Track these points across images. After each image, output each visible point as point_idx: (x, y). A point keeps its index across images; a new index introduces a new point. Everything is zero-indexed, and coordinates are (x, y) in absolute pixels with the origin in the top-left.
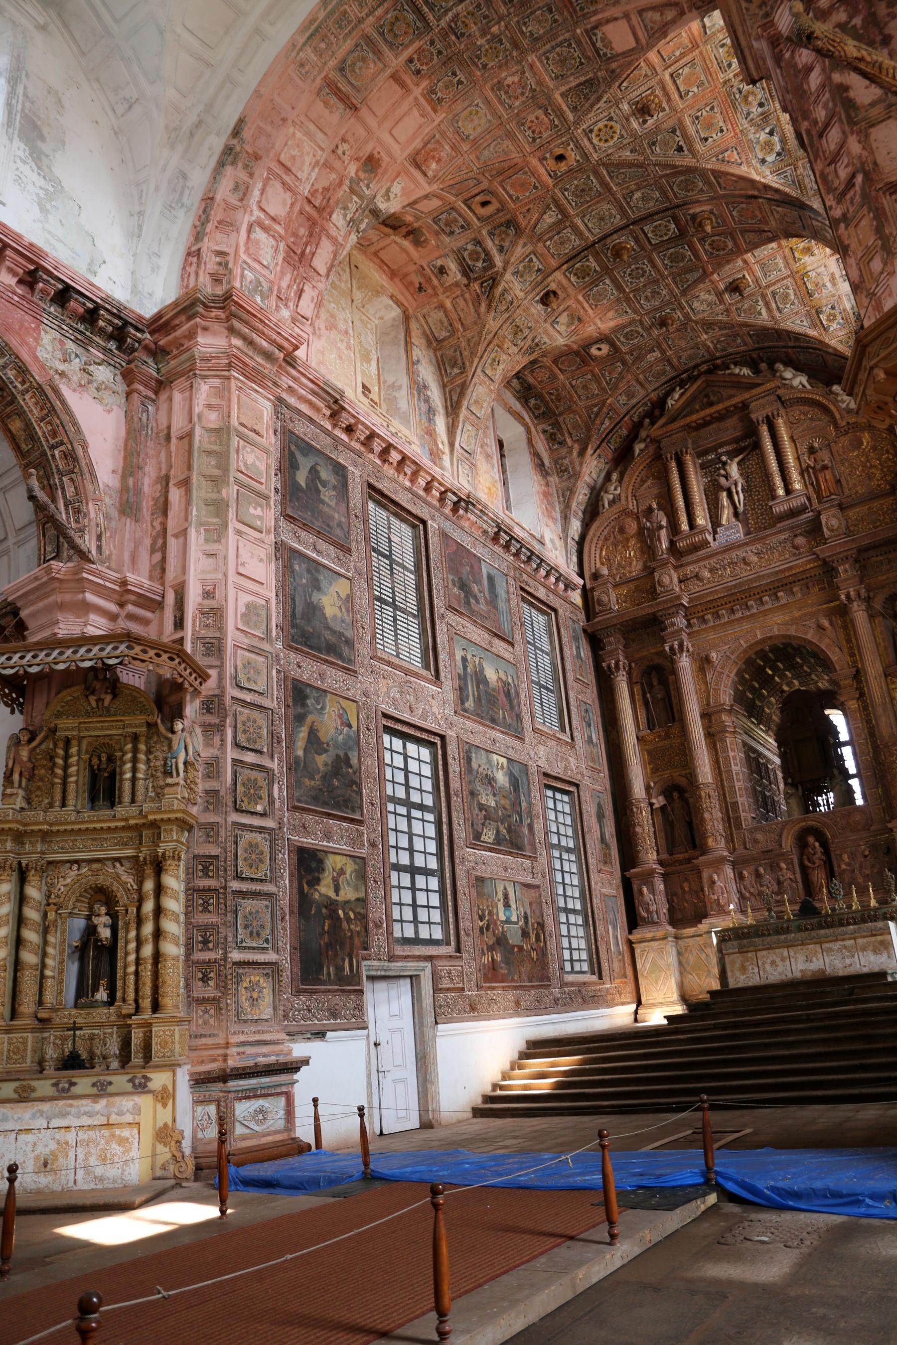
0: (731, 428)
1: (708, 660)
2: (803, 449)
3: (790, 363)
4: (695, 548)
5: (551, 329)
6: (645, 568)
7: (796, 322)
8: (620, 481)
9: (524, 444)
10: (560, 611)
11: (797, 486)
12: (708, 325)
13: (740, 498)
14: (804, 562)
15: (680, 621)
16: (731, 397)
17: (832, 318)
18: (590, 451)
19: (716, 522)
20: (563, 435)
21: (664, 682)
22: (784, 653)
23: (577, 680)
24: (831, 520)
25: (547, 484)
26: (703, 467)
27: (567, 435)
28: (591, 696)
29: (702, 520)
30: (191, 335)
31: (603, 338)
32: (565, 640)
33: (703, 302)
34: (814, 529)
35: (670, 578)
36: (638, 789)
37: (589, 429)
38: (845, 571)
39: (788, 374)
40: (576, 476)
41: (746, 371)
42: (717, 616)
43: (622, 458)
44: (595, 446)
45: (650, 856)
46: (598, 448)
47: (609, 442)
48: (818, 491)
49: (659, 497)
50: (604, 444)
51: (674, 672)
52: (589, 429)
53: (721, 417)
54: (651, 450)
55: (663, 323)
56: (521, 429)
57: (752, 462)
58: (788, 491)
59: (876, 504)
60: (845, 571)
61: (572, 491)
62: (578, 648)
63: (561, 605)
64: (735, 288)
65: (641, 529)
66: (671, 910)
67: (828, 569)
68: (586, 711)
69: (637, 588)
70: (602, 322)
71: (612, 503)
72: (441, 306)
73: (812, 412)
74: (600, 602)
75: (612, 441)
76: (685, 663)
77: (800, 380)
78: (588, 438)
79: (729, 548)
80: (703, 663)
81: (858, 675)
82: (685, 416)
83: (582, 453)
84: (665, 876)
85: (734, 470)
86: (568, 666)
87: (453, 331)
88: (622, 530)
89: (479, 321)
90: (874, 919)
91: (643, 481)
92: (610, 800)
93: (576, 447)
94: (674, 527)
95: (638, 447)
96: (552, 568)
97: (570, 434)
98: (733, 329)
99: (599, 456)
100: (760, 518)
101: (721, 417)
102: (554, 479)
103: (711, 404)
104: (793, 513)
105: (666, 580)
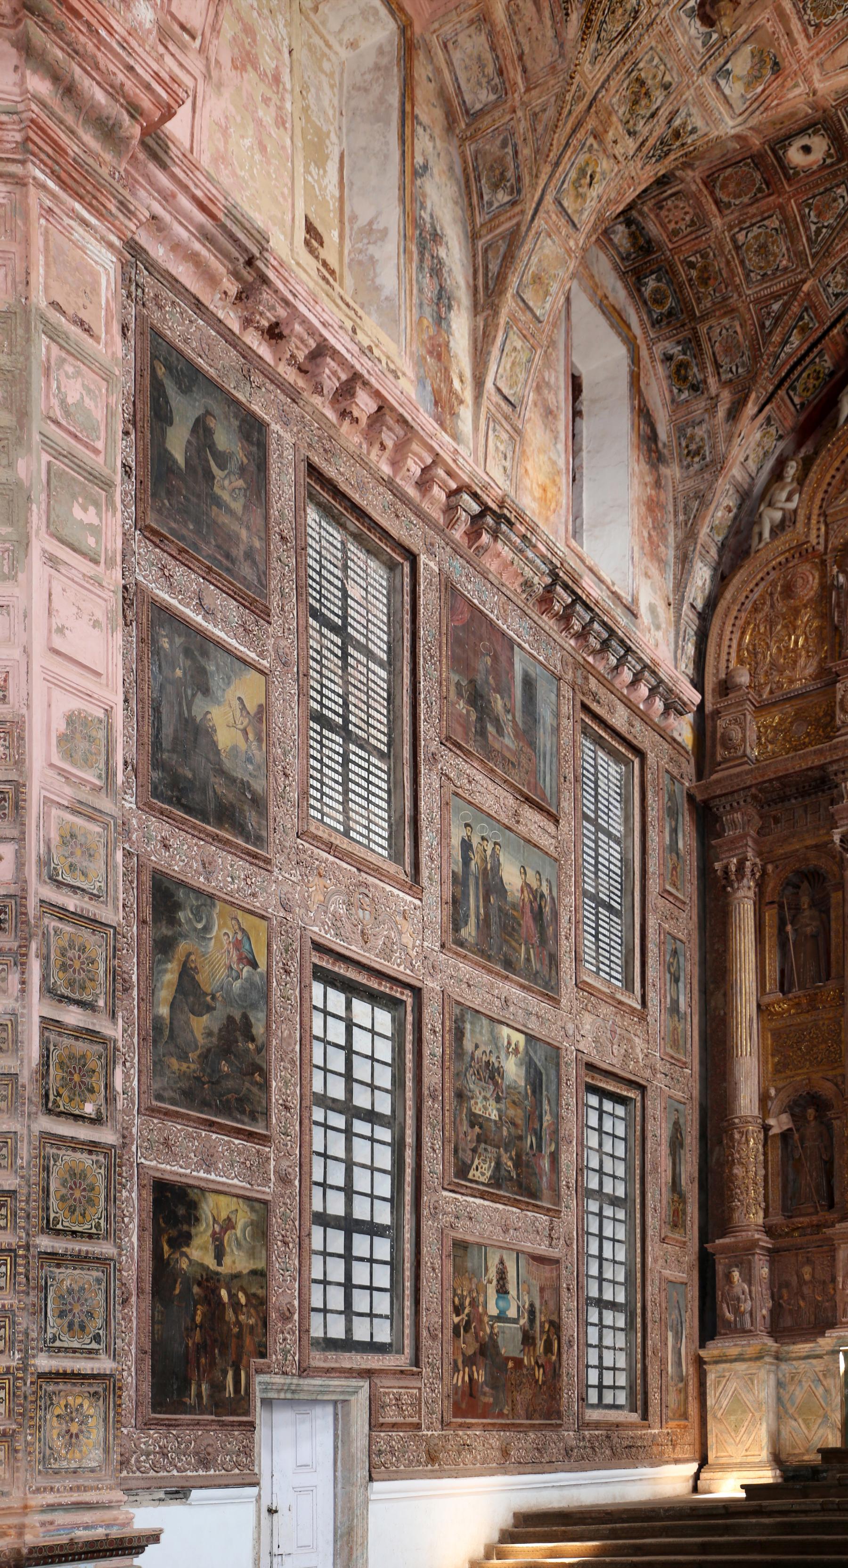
5: (711, 90)
9: (623, 386)
10: (651, 757)
18: (751, 408)
20: (703, 369)
23: (664, 894)
25: (658, 484)
27: (710, 369)
28: (685, 925)
32: (652, 814)
44: (762, 400)
46: (768, 401)
47: (792, 387)
50: (782, 393)
52: (756, 357)
56: (620, 351)
62: (674, 831)
63: (654, 745)
66: (776, 1312)
68: (675, 953)
75: (799, 386)
78: (753, 376)
84: (773, 1254)
86: (653, 866)
92: (696, 1116)
93: (726, 397)
96: (646, 666)
97: (717, 366)
99: (768, 420)
102: (672, 472)
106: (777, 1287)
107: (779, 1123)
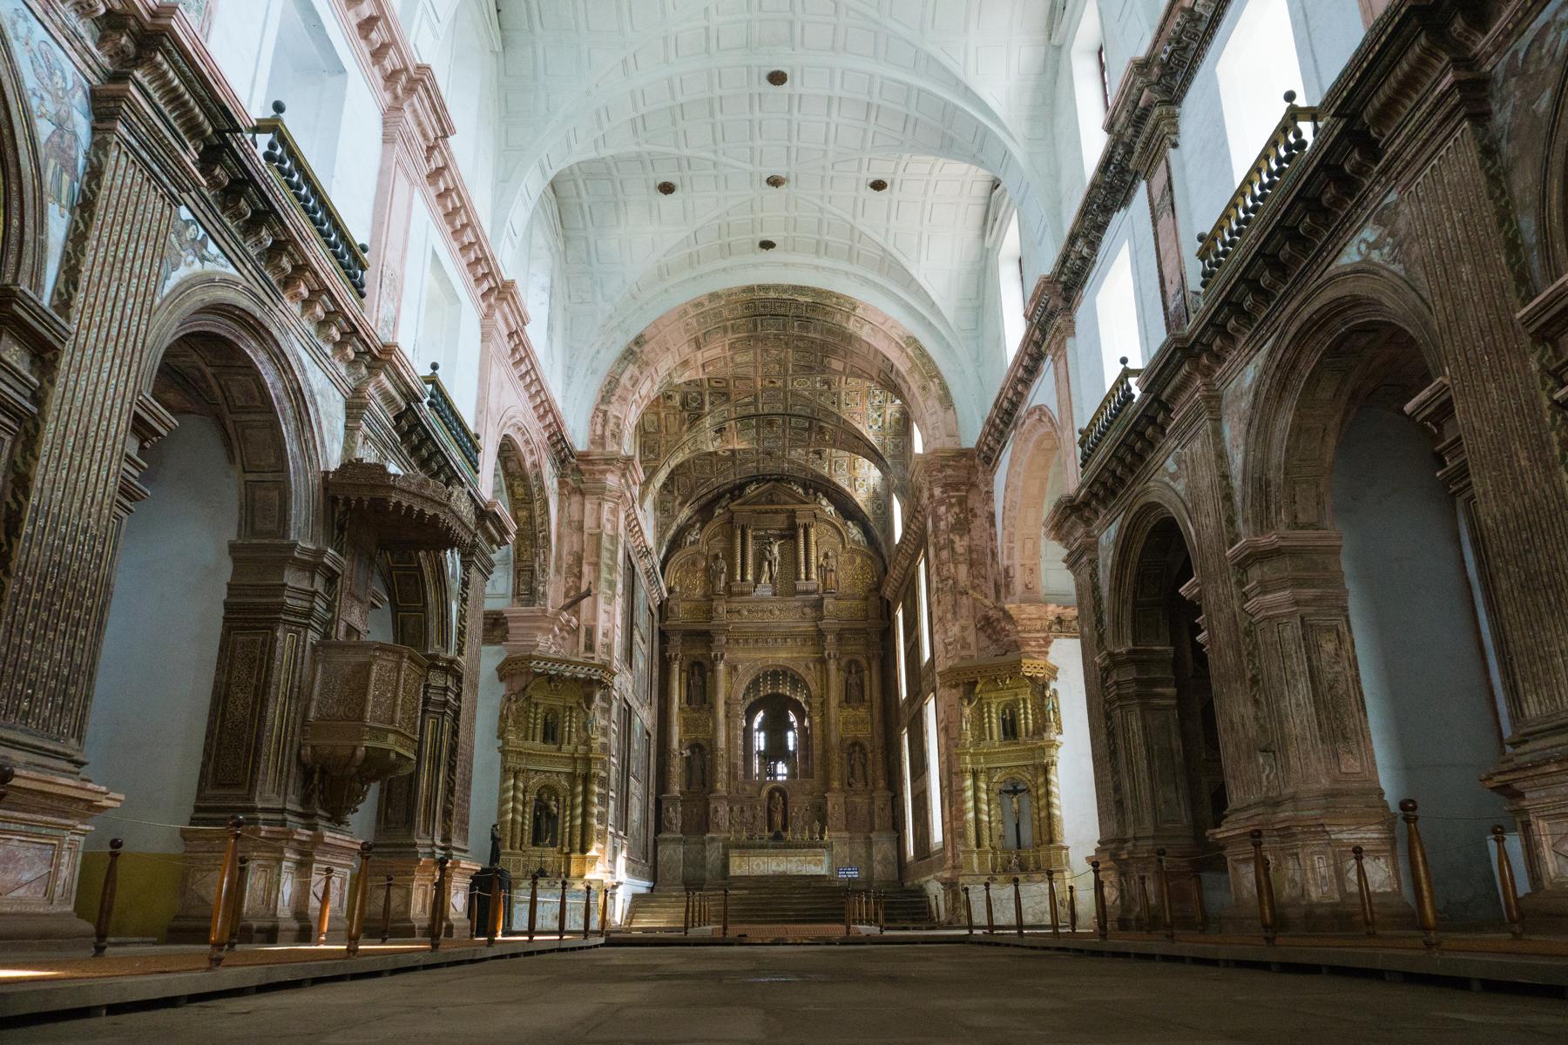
0: (781, 521)
1: (735, 668)
2: (821, 553)
3: (826, 495)
4: (742, 594)
6: (705, 595)
7: (842, 481)
8: (701, 530)
11: (814, 576)
12: (791, 462)
13: (776, 569)
14: (807, 626)
15: (724, 639)
16: (786, 503)
17: (861, 486)
19: (757, 580)
21: (703, 676)
22: (777, 674)
24: (828, 602)
26: (755, 538)
29: (749, 577)
30: (603, 472)
31: (733, 452)
33: (797, 454)
34: (818, 606)
35: (721, 608)
36: (675, 744)
37: (692, 492)
38: (830, 638)
39: (824, 502)
40: (674, 517)
41: (800, 490)
42: (746, 641)
43: (705, 513)
45: (676, 789)
48: (825, 584)
49: (723, 549)
51: (713, 671)
53: (776, 512)
54: (727, 515)
55: (769, 454)
57: (787, 547)
58: (807, 578)
59: (854, 603)
60: (830, 638)
61: (668, 528)
64: (819, 453)
65: (707, 569)
67: (821, 634)
69: (696, 608)
70: (739, 444)
71: (692, 543)
72: (657, 414)
73: (832, 531)
74: (672, 611)
76: (721, 667)
77: (830, 509)
78: (691, 495)
79: (762, 600)
80: (733, 669)
81: (824, 703)
82: (755, 504)
83: (682, 504)
85: (776, 549)
87: (658, 431)
88: (694, 564)
89: (679, 433)
90: (815, 847)
91: (715, 536)
94: (731, 575)
95: (718, 511)
98: (803, 469)
100: (788, 587)
101: (776, 512)
103: (772, 502)
104: (807, 592)
105: (720, 610)
106: (684, 814)
107: (686, 753)
